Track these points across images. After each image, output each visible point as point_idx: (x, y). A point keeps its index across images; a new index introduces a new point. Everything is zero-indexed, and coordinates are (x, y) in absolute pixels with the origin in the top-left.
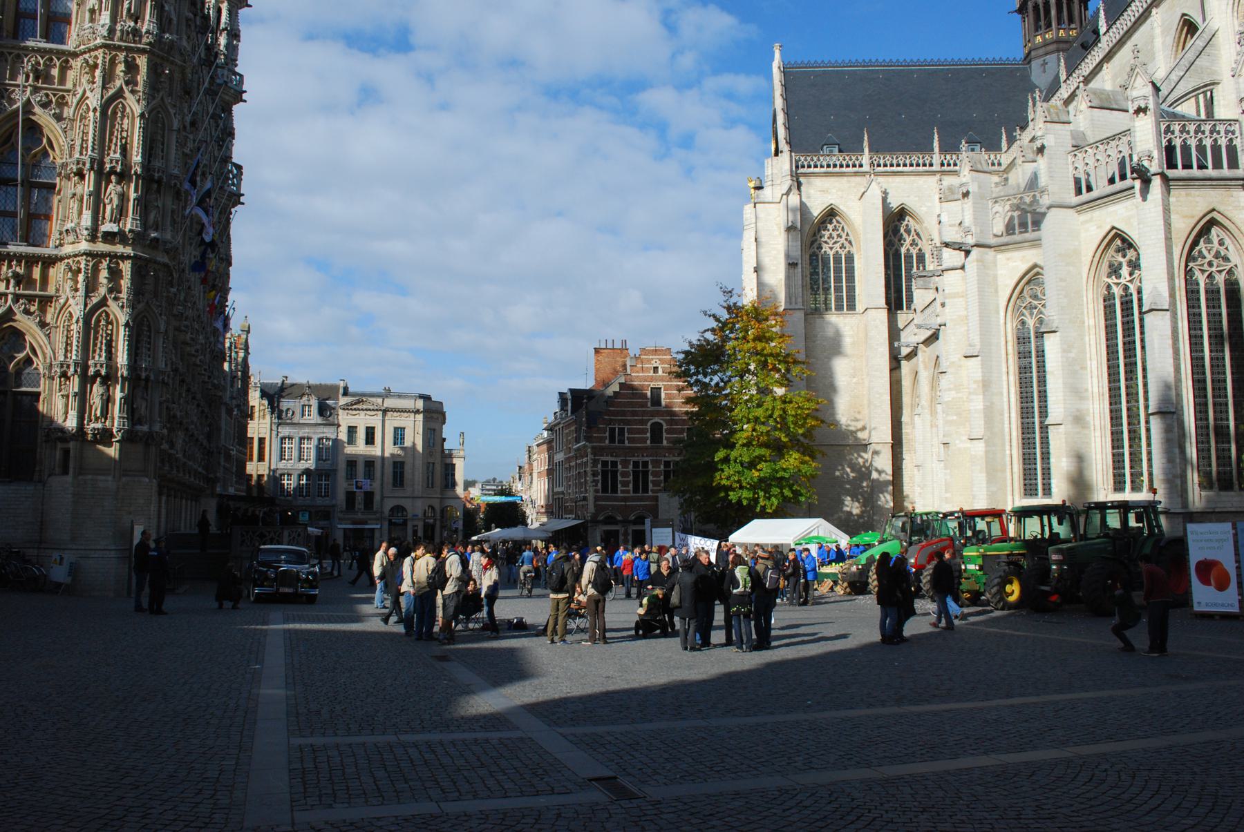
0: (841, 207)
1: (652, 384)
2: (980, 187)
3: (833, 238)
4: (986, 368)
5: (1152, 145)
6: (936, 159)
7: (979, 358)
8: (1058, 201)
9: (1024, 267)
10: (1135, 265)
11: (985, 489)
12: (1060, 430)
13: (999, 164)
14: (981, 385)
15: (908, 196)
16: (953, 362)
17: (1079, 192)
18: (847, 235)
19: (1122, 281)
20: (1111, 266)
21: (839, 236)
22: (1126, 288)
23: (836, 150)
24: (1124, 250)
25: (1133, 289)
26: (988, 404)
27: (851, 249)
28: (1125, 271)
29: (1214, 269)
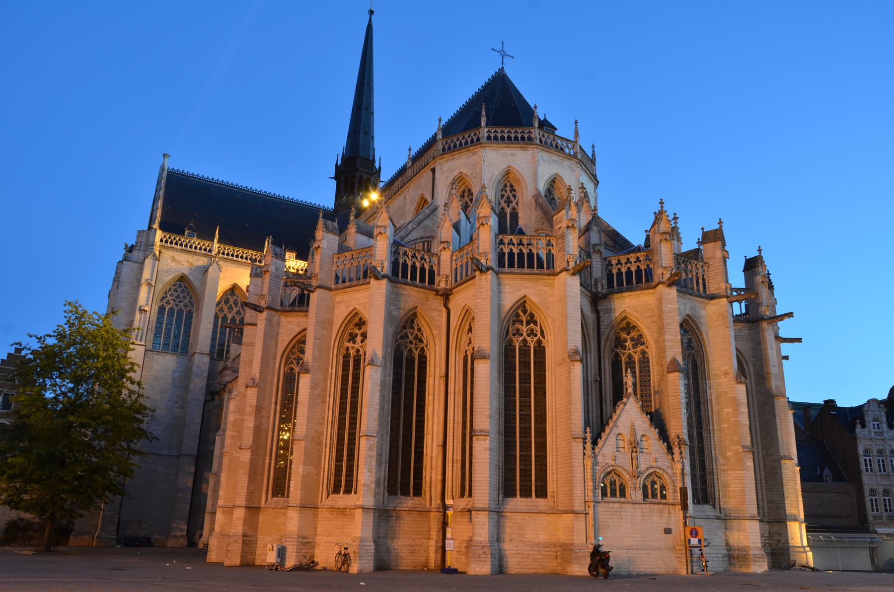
1: (5, 390)
2: (276, 269)
3: (180, 298)
4: (260, 397)
5: (384, 258)
8: (322, 283)
9: (298, 330)
10: (364, 336)
11: (246, 488)
12: (301, 445)
14: (254, 409)
16: (241, 392)
17: (337, 282)
18: (191, 298)
19: (356, 346)
20: (351, 334)
22: (358, 351)
24: (360, 325)
25: (361, 353)
26: (258, 424)
27: (192, 309)
28: (359, 339)
29: (413, 346)
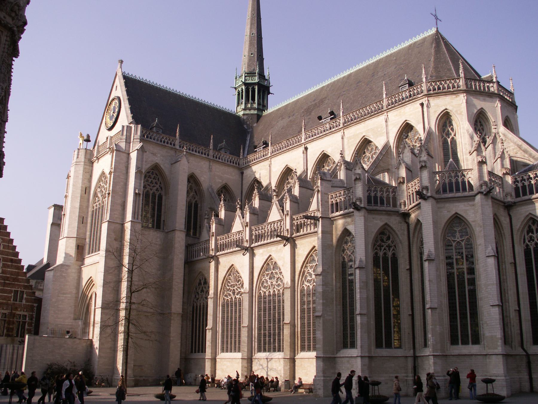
0: (162, 166)
3: (153, 184)
6: (211, 153)
7: (365, 269)
9: (381, 224)
13: (239, 164)
15: (196, 169)
18: (160, 183)
21: (156, 183)
23: (161, 132)
28: (458, 235)
